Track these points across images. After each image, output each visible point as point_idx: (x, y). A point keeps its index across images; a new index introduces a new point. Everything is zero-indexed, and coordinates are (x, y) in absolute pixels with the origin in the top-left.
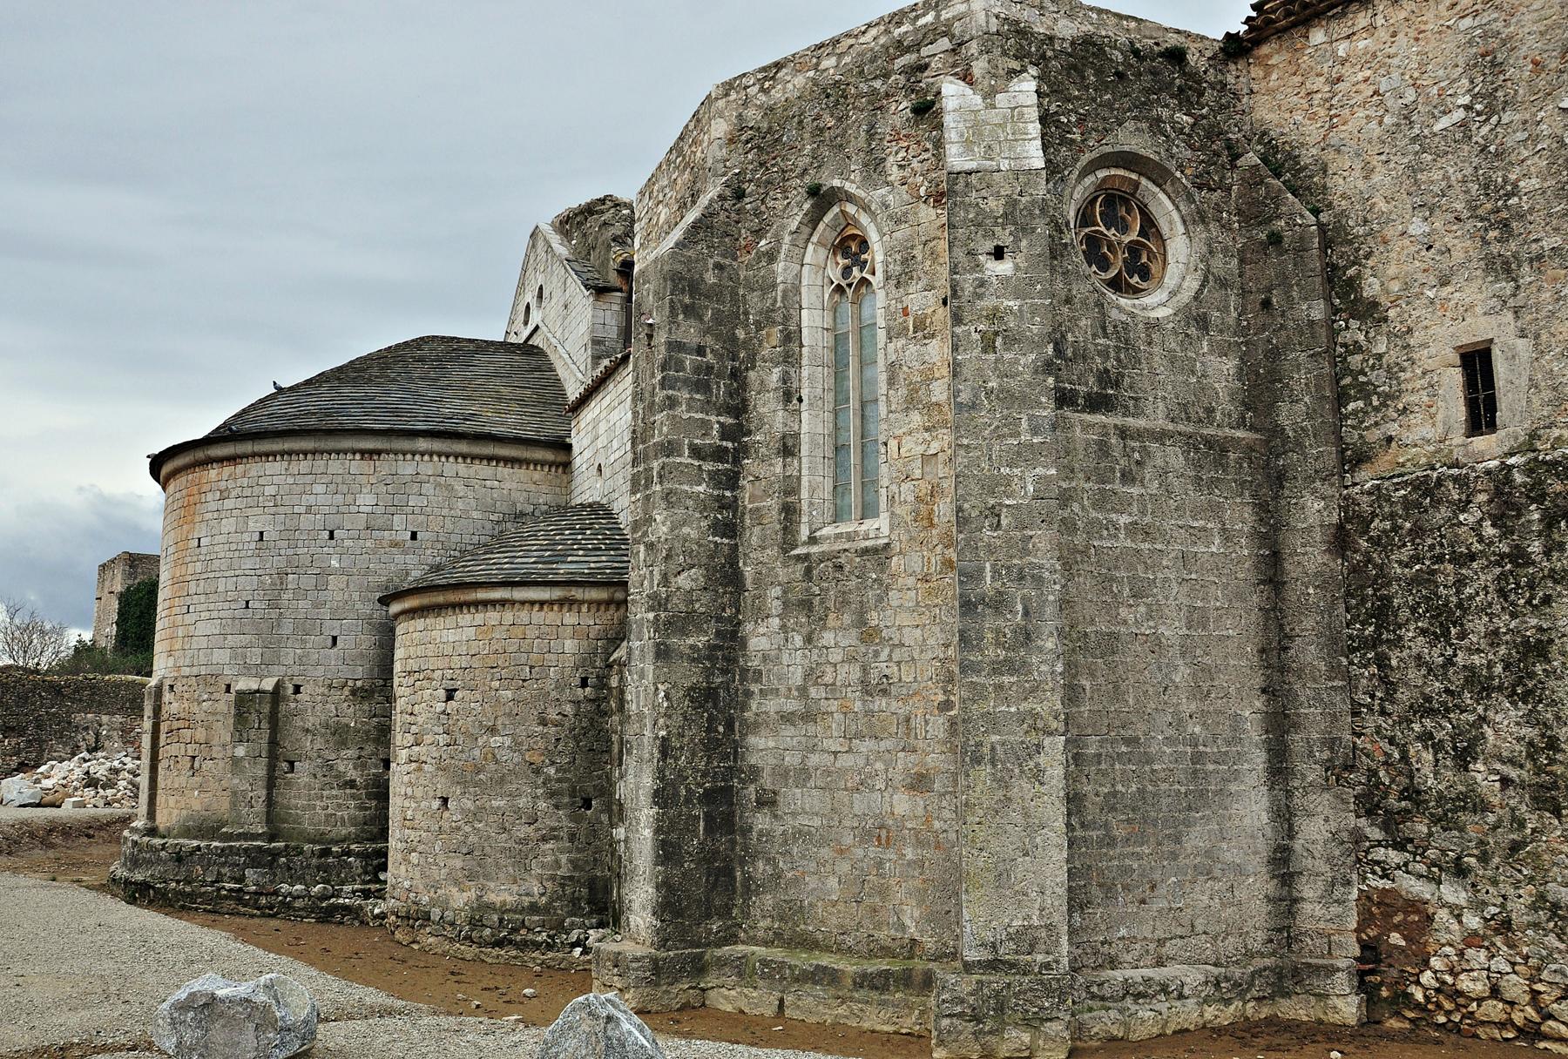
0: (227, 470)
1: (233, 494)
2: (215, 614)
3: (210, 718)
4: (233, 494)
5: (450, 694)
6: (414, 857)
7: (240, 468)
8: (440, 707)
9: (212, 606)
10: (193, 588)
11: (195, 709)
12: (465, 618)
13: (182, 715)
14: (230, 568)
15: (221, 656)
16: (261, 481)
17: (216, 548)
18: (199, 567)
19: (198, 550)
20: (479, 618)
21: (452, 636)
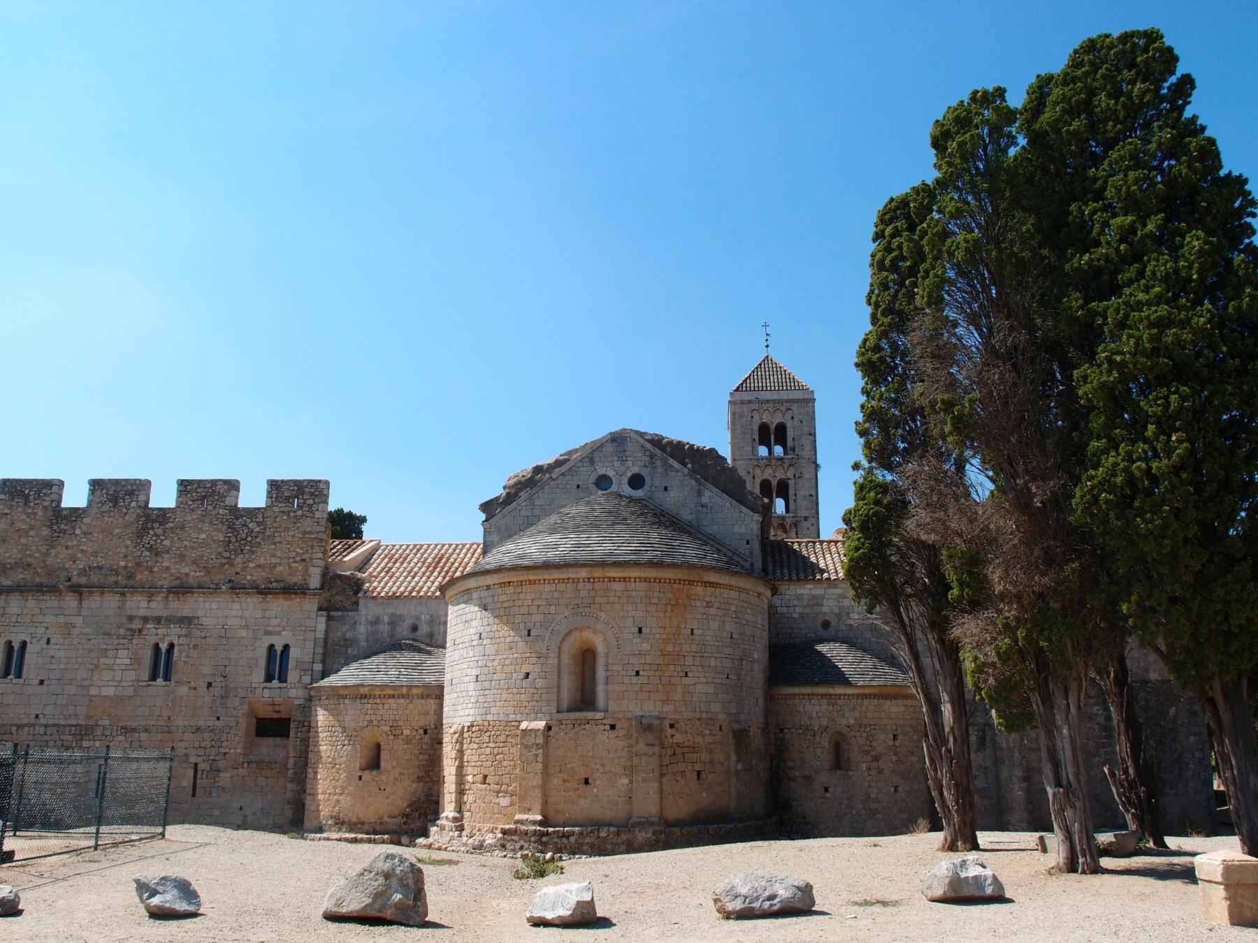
0: (710, 590)
1: (716, 605)
2: (710, 680)
3: (712, 746)
4: (716, 605)
5: (895, 737)
6: (879, 817)
7: (718, 590)
8: (891, 743)
9: (707, 675)
10: (689, 661)
11: (699, 739)
12: (900, 702)
13: (686, 744)
14: (717, 652)
15: (716, 707)
16: (730, 601)
17: (708, 638)
18: (694, 648)
19: (691, 637)
20: (905, 702)
21: (895, 709)
